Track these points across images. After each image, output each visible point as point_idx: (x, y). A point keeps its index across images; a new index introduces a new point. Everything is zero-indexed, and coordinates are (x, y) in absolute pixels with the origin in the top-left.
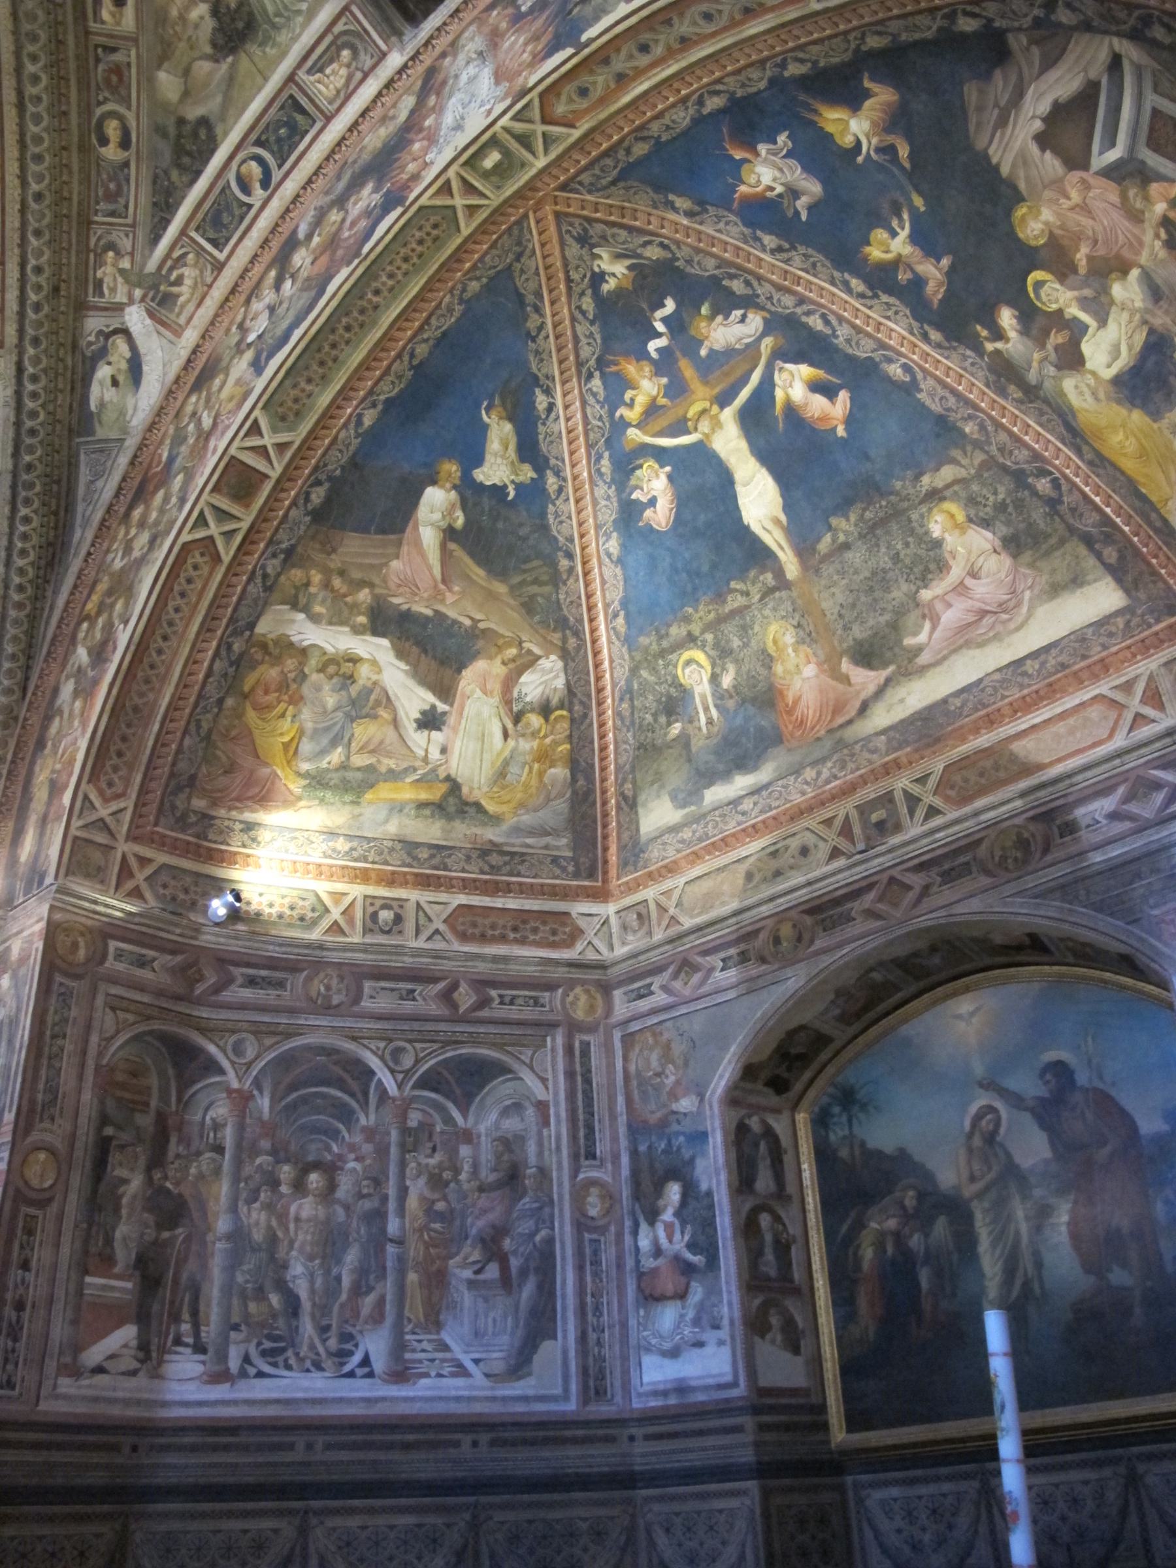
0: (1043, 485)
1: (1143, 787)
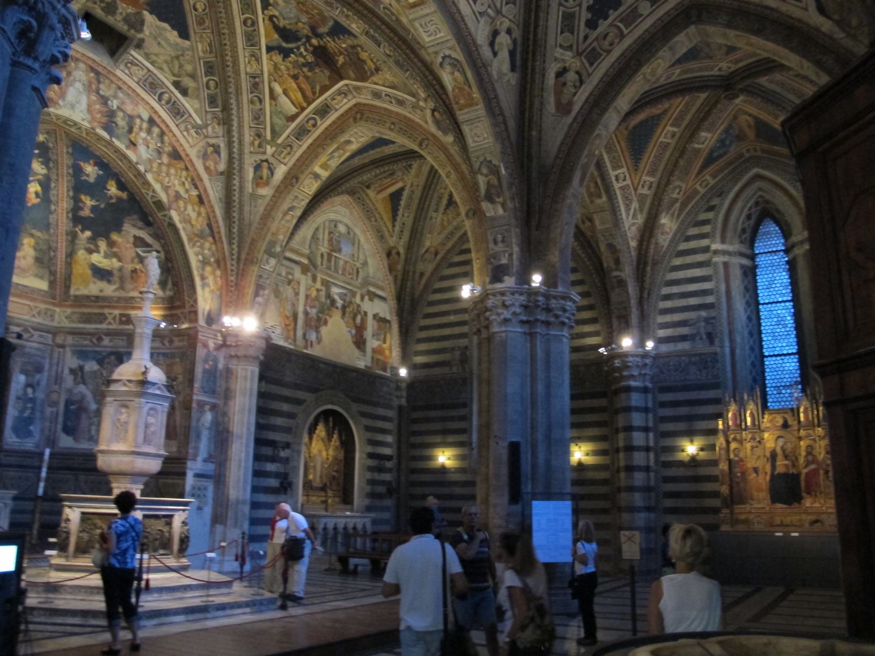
0: (52, 254)
1: (26, 330)
